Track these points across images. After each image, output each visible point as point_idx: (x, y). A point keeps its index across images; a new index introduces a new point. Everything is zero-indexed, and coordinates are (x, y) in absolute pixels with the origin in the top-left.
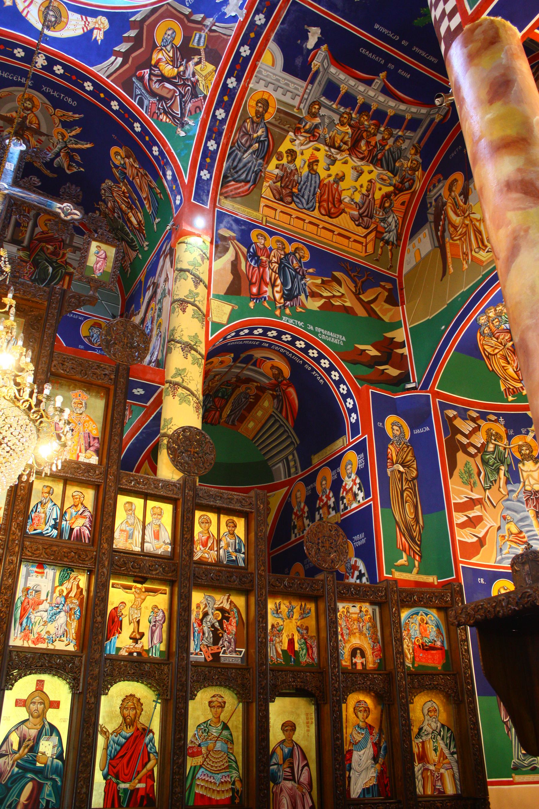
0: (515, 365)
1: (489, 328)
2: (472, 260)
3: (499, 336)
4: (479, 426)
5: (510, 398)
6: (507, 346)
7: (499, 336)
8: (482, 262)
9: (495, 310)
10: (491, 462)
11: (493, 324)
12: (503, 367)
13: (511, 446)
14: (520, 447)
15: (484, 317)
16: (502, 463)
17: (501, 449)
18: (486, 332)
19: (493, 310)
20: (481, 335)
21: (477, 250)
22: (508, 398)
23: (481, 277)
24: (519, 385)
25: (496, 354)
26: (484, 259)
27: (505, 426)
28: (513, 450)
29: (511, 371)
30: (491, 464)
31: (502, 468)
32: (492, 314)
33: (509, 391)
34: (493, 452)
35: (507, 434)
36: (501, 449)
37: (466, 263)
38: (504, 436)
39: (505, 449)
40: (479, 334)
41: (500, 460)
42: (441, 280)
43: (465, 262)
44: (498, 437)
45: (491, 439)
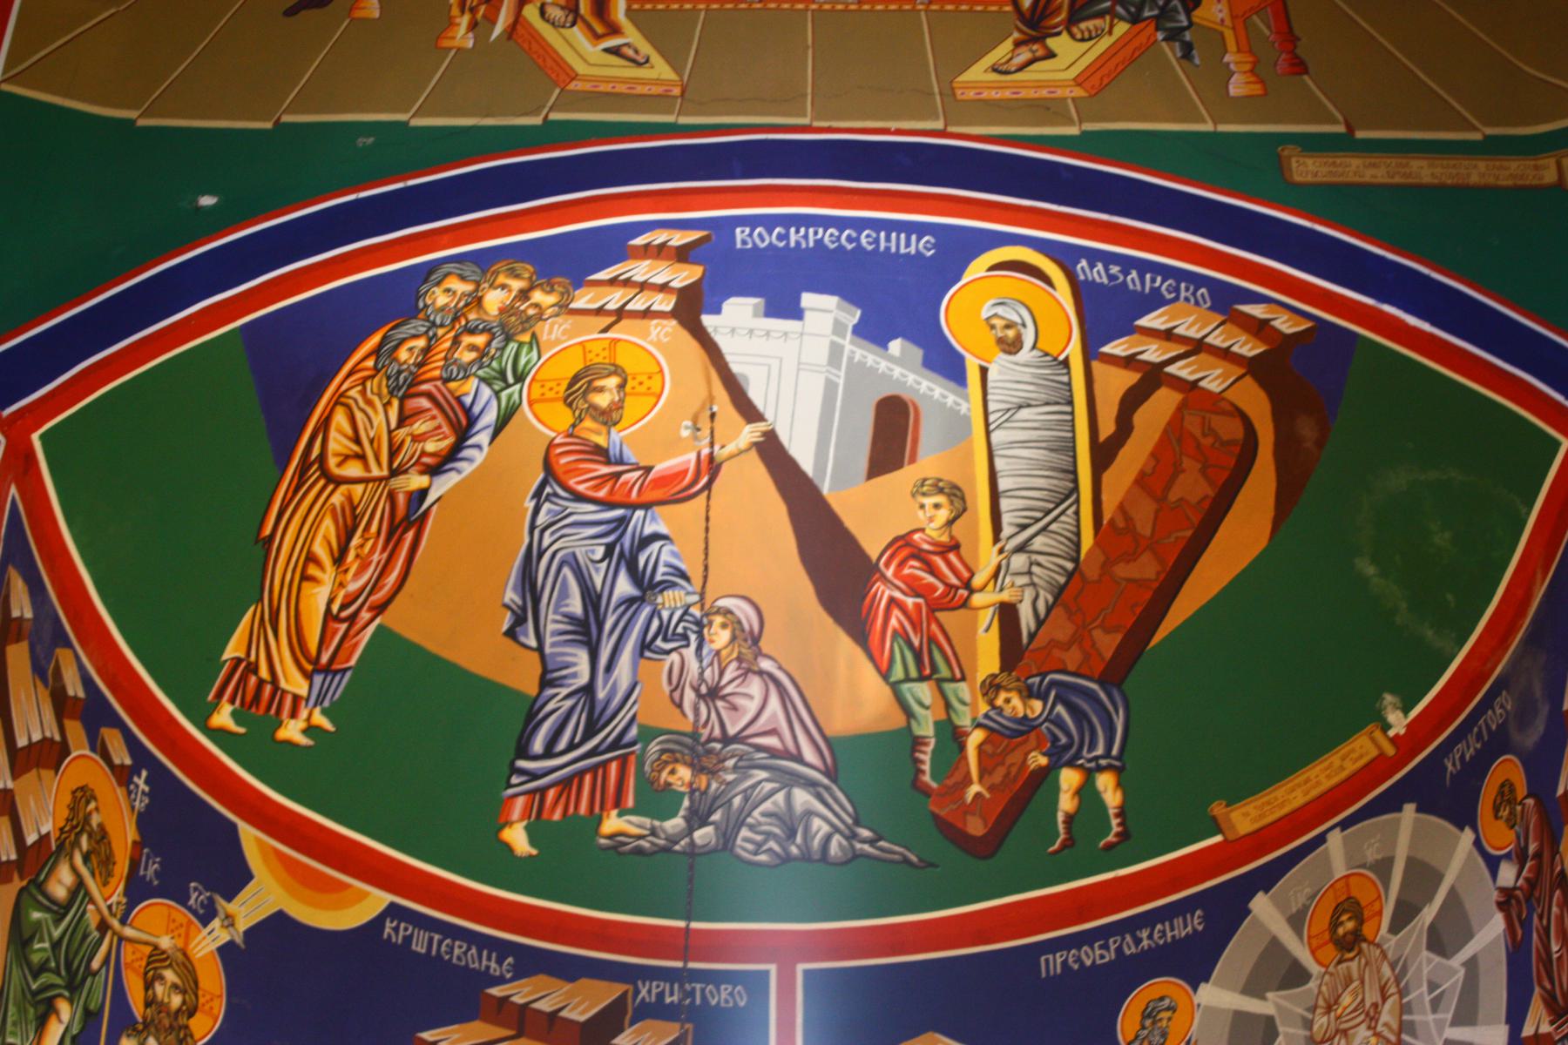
0: (353, 587)
1: (427, 350)
2: (511, 31)
3: (420, 412)
4: (63, 750)
5: (223, 717)
6: (397, 482)
7: (420, 412)
8: (574, 76)
9: (524, 295)
10: (41, 947)
11: (456, 341)
12: (311, 558)
13: (128, 932)
14: (158, 958)
15: (462, 287)
16: (73, 987)
17: (92, 919)
18: (403, 354)
19: (517, 285)
20: (376, 352)
21: (556, 13)
22: (214, 707)
23: (537, 121)
24: (294, 682)
25: (339, 481)
26: (580, 68)
27: (143, 821)
28: (128, 953)
29: (317, 598)
30: (36, 958)
31: (64, 1009)
32: (494, 300)
33: (244, 679)
34: (59, 910)
35: (134, 864)
36: (92, 919)
37: (473, 26)
38: (122, 867)
39: (103, 927)
40: (375, 339)
41: (68, 965)
42: (291, 12)
43: (465, 21)
44: (100, 858)
45: (76, 843)
